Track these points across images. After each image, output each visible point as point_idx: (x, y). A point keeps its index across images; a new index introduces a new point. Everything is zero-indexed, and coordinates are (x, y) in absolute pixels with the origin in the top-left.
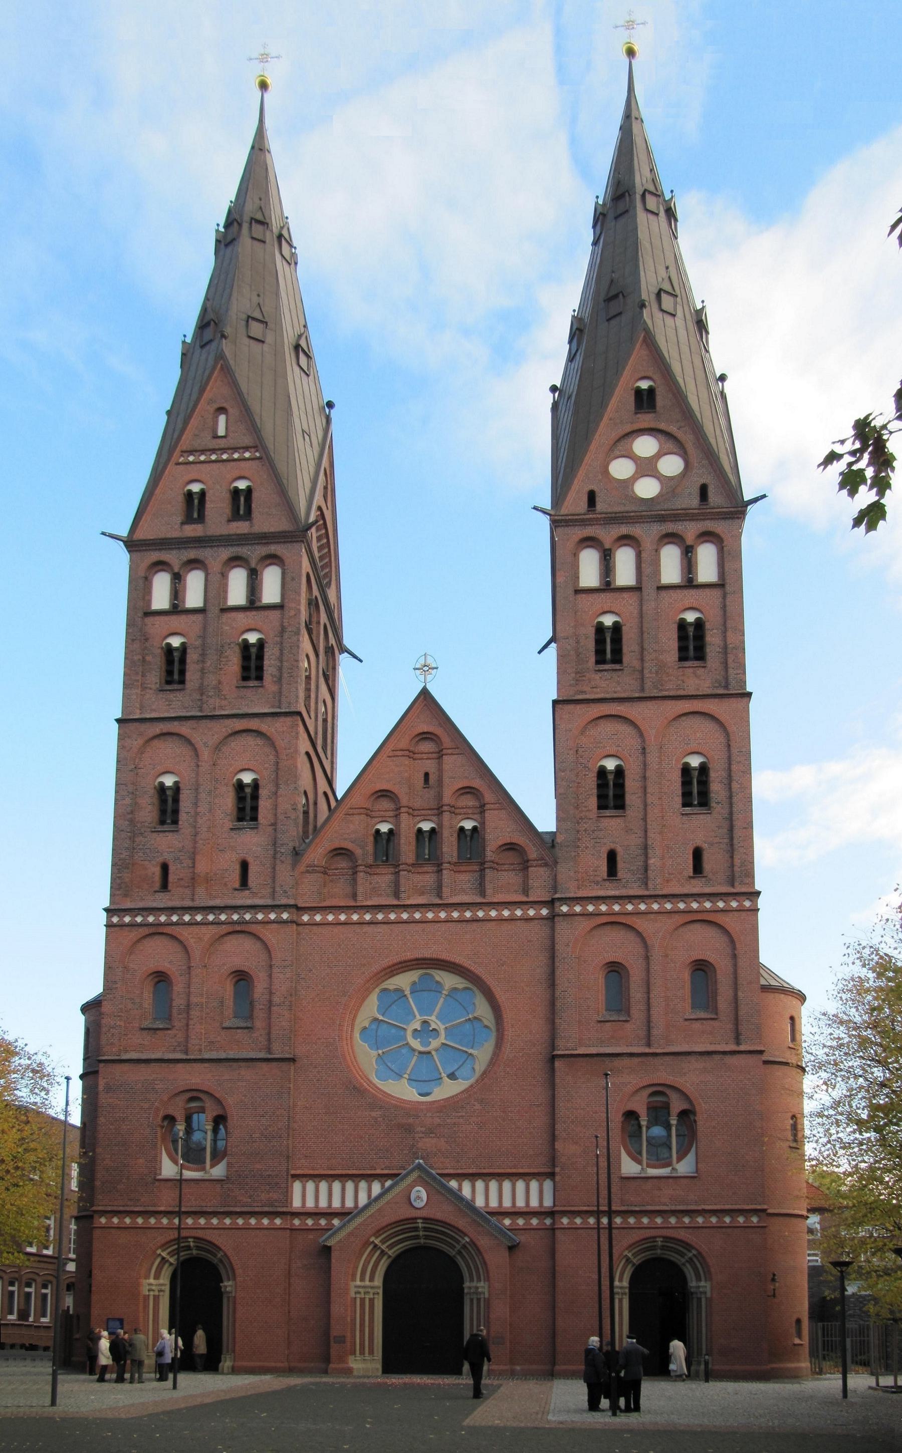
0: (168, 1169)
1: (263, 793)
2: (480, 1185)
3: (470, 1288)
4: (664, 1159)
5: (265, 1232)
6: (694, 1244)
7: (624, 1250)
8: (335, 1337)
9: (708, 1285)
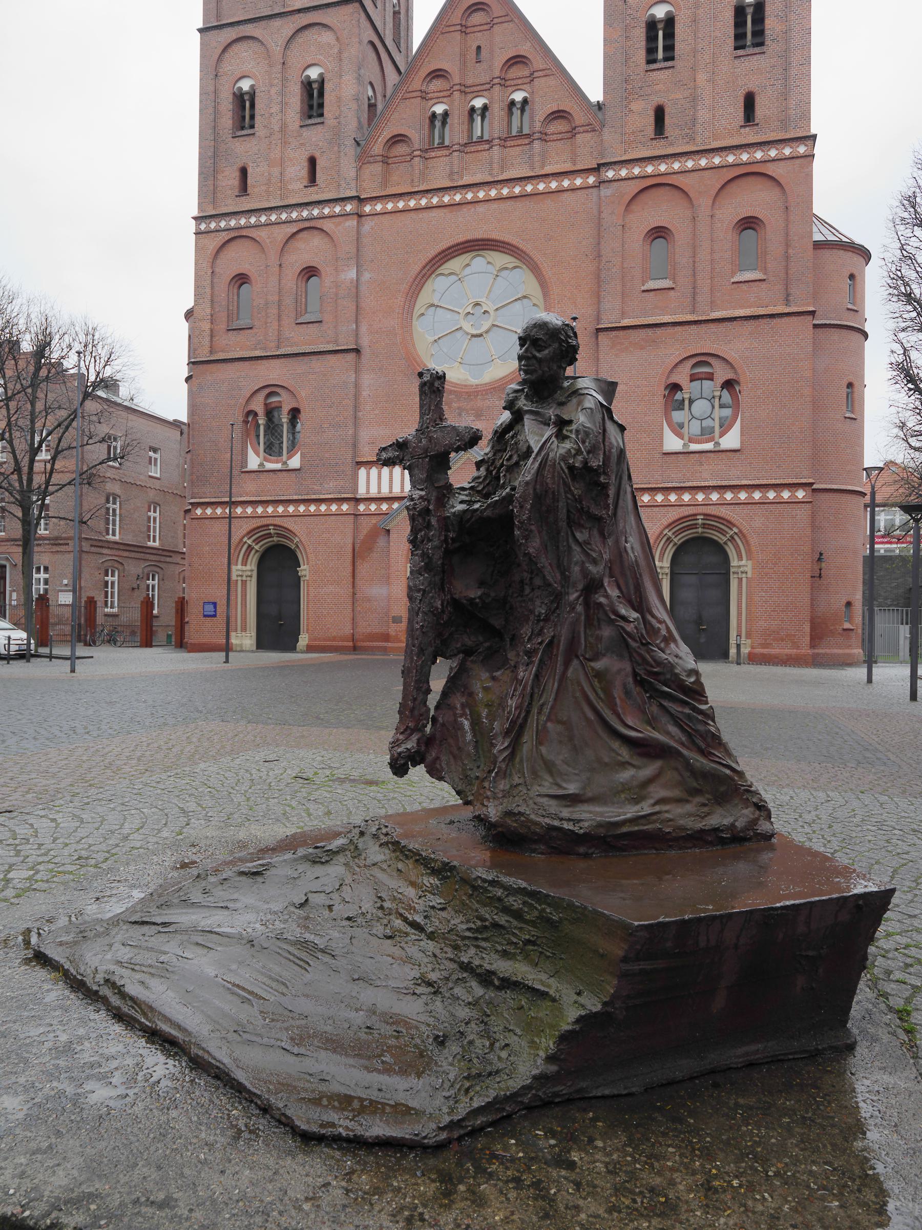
0: (253, 461)
1: (328, 87)
5: (333, 518)
7: (664, 529)
8: (393, 617)
9: (750, 563)
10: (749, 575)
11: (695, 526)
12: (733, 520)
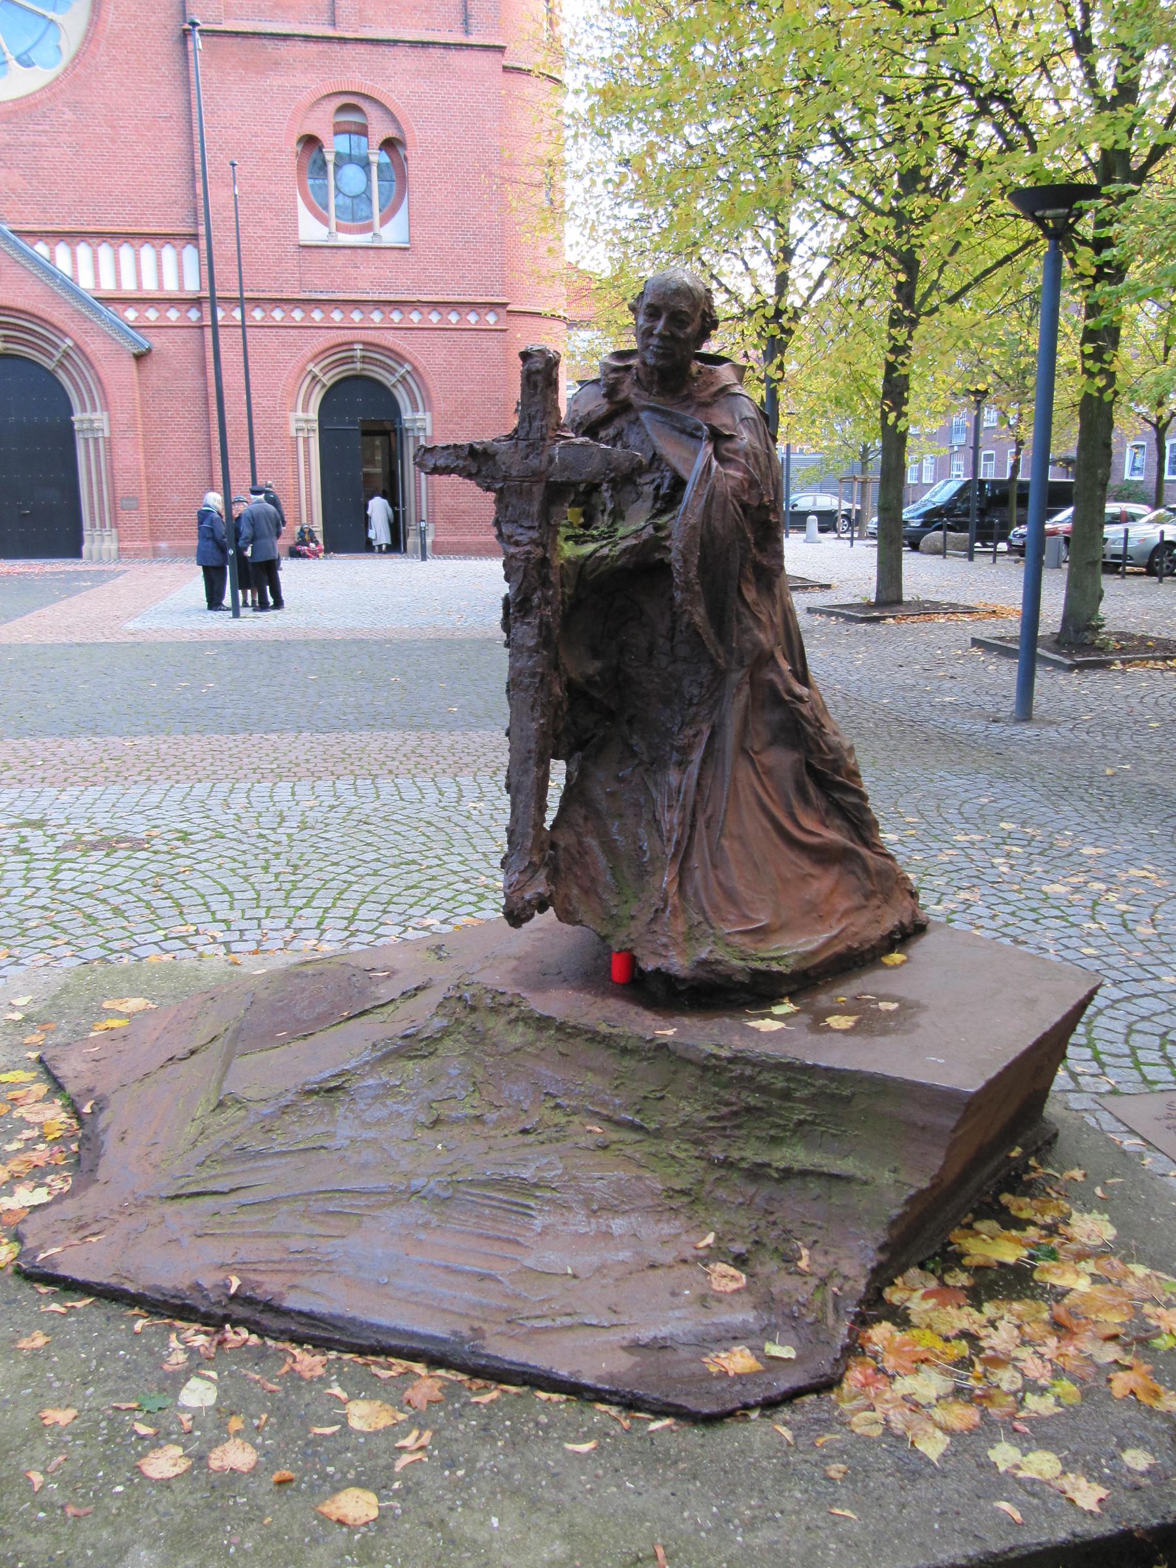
2: (83, 251)
3: (82, 421)
4: (361, 219)
6: (408, 356)
9: (428, 417)
10: (429, 433)
11: (350, 360)
12: (404, 353)
